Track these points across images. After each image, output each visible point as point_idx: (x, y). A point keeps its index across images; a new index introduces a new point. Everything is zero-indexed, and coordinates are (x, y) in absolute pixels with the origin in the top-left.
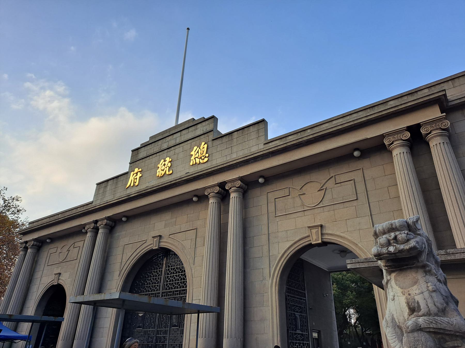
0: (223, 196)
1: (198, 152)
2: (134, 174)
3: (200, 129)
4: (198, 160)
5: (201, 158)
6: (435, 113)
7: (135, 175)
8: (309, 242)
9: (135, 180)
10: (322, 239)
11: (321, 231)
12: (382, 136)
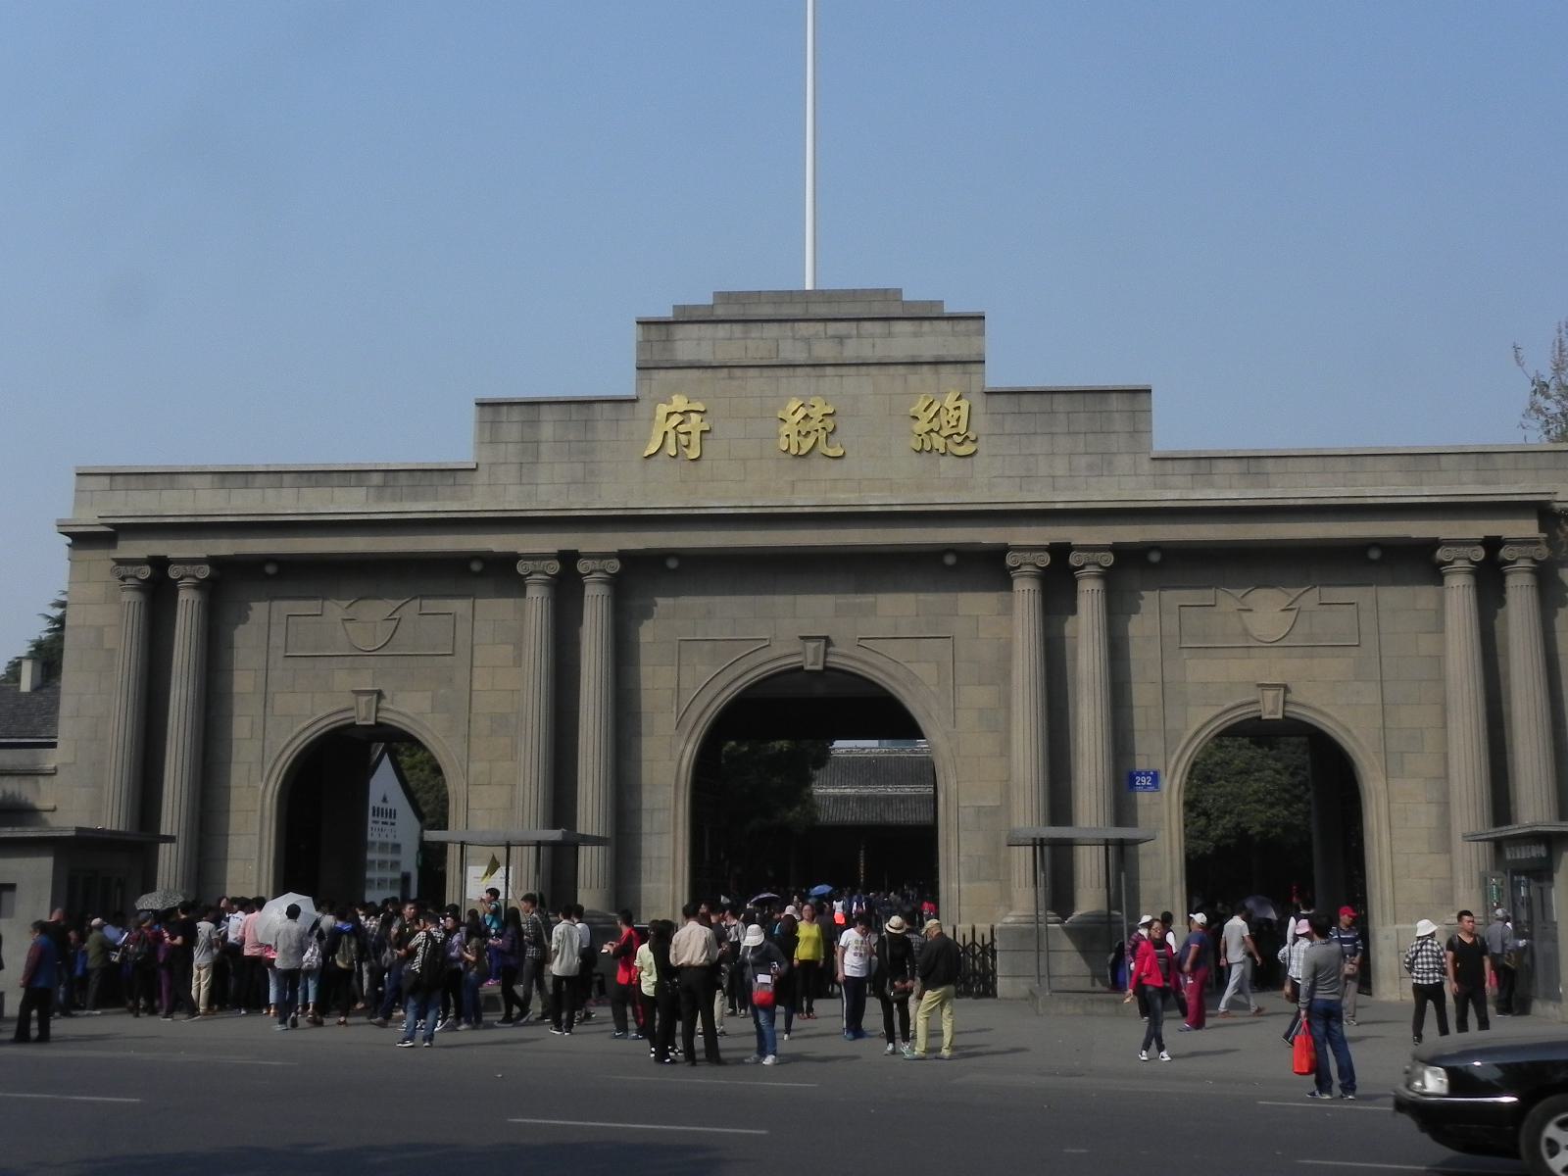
0: (1058, 579)
1: (937, 413)
2: (670, 414)
3: (932, 342)
4: (938, 442)
5: (951, 436)
6: (1528, 528)
7: (675, 420)
8: (1256, 714)
9: (683, 438)
10: (1284, 711)
11: (1285, 696)
12: (1435, 544)
